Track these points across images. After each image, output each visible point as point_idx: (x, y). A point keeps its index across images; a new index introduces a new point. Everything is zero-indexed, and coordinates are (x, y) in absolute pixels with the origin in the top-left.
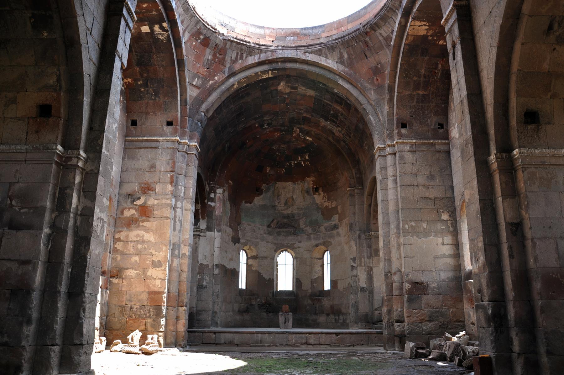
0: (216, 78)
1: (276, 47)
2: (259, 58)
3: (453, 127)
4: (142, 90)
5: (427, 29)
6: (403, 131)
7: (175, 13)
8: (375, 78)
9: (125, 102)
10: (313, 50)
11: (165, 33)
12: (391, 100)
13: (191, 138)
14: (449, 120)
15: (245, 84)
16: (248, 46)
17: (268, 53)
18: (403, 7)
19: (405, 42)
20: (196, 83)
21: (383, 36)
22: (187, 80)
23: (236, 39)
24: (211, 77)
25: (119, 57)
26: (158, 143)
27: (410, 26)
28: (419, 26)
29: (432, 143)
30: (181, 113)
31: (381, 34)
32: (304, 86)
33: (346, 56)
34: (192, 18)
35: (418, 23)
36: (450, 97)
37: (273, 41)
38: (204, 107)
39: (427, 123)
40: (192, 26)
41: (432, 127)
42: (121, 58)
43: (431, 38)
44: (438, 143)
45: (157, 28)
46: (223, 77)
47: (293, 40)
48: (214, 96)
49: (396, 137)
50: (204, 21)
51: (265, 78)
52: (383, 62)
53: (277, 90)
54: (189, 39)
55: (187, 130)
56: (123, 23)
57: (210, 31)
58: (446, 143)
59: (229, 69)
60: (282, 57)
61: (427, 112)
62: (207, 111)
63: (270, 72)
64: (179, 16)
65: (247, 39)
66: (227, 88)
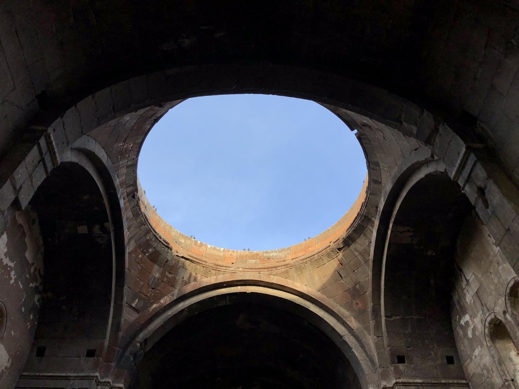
0: (162, 301)
1: (235, 268)
2: (216, 279)
3: (469, 360)
4: (64, 307)
5: (411, 236)
6: (401, 366)
7: (122, 213)
8: (355, 302)
9: (36, 323)
10: (279, 272)
11: (106, 235)
12: (378, 326)
13: (117, 378)
14: (459, 351)
15: (197, 313)
16: (204, 266)
17: (226, 274)
18: (381, 211)
19: (387, 252)
20: (136, 305)
21: (358, 251)
22: (125, 299)
23: (190, 256)
24: (157, 299)
25: (14, 188)
26: (67, 381)
27: (392, 232)
28: (402, 232)
29: (445, 384)
30: (109, 341)
31: (356, 250)
33: (317, 278)
34: (141, 225)
35: (401, 229)
36: (453, 321)
37: (232, 264)
38: (141, 336)
39: (430, 356)
40: (141, 234)
41: (439, 362)
42: (17, 191)
44: (452, 383)
45: (96, 229)
46: (170, 299)
47: (255, 263)
48: (158, 322)
49: (392, 375)
50: (156, 232)
51: (221, 305)
52: (362, 280)
54: (134, 251)
55: (113, 364)
56: (35, 151)
57: (161, 245)
58: (463, 384)
59: (179, 291)
60: (242, 279)
61: (427, 342)
62: (146, 341)
63: (228, 298)
64: (127, 219)
65: (204, 259)
66: (174, 314)
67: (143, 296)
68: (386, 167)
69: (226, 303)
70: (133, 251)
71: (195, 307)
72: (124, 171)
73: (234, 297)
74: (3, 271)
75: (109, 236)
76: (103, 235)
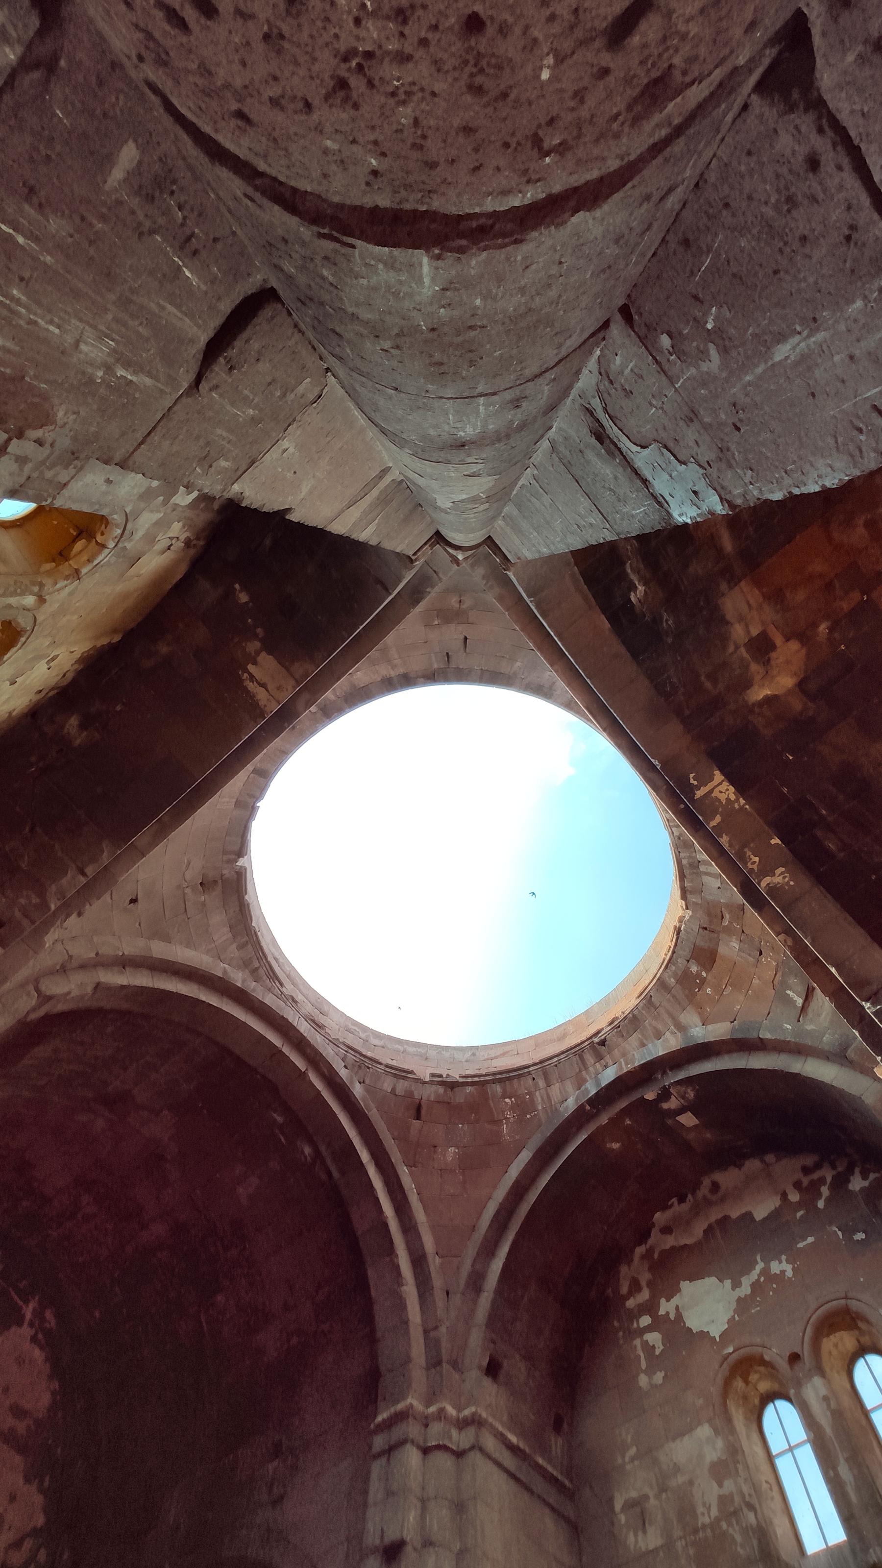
5: (255, 663)
15: (776, 841)
28: (263, 685)
32: (724, 639)
35: (261, 695)
43: (259, 630)
45: (673, 1103)
51: (732, 789)
53: (801, 685)
67: (778, 978)
68: (224, 803)
69: (720, 784)
70: (699, 1013)
71: (757, 859)
72: (555, 1091)
73: (692, 781)
74: (758, 1299)
75: (670, 1087)
76: (676, 1094)
